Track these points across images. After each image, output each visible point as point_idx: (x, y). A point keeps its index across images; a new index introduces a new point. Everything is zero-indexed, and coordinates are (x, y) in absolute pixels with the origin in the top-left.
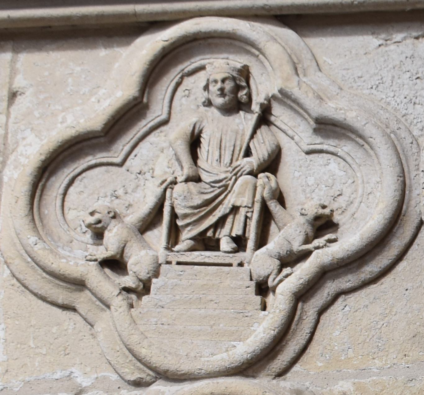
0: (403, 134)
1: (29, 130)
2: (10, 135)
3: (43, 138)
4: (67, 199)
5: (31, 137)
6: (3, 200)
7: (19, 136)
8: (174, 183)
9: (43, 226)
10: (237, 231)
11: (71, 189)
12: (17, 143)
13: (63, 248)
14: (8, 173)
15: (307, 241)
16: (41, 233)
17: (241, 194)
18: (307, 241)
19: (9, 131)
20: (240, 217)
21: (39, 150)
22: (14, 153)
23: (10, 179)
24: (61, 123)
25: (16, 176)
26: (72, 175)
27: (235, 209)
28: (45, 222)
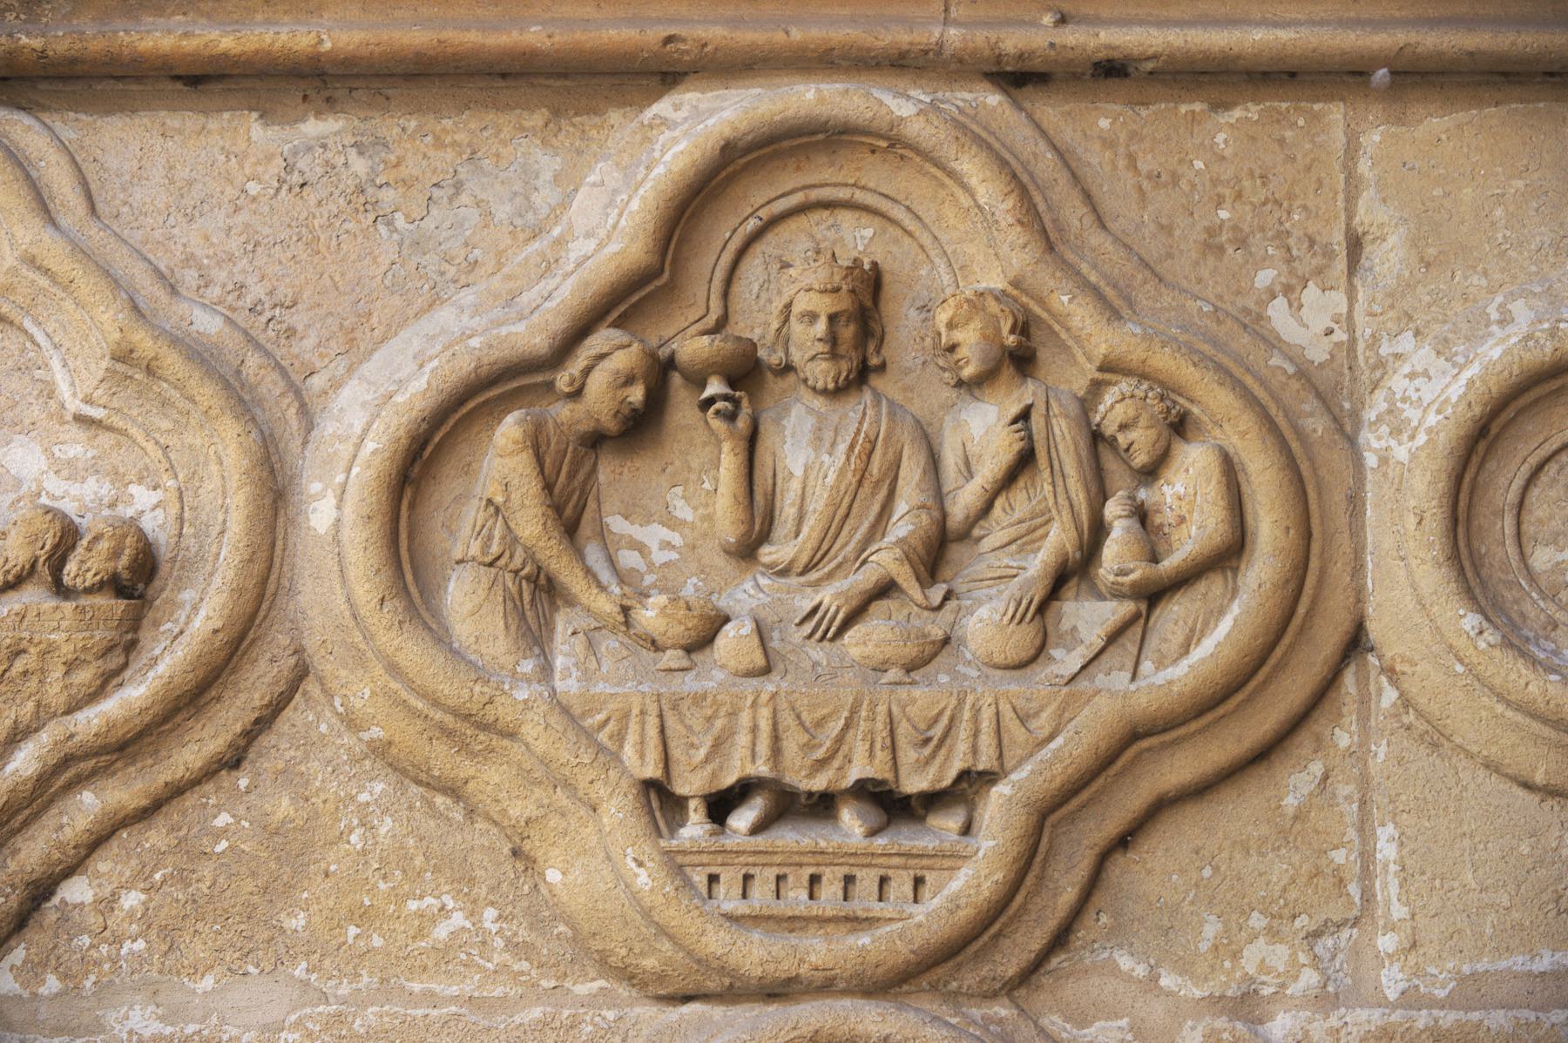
1: (1409, 334)
2: (1361, 346)
3: (1460, 359)
4: (1525, 517)
5: (1423, 356)
6: (1369, 513)
7: (1384, 350)
9: (1484, 585)
11: (1535, 492)
12: (1381, 364)
13: (1538, 645)
14: (1375, 444)
16: (1483, 603)
19: (1358, 333)
21: (1465, 394)
22: (1380, 395)
23: (1384, 460)
24: (1502, 322)
25: (1401, 453)
26: (1533, 460)
28: (1484, 572)
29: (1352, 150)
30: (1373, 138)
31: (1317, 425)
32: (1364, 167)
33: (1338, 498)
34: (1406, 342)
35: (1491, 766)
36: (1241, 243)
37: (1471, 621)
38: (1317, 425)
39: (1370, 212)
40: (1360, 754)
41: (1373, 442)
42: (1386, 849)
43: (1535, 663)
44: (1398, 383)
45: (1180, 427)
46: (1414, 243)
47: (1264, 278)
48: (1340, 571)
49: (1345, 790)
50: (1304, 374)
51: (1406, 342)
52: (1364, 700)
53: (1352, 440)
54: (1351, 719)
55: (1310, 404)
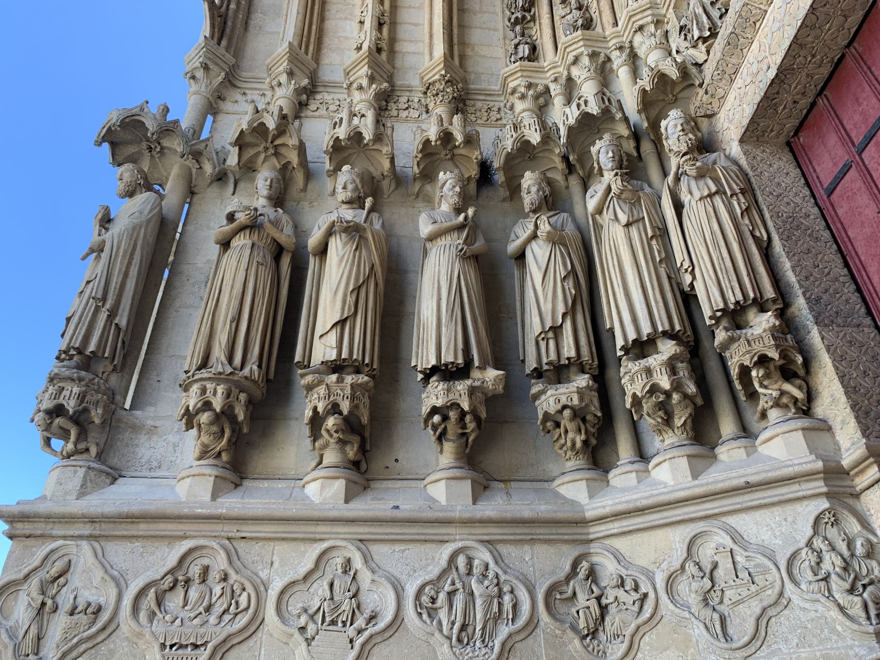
0: (399, 586)
5: (278, 579)
8: (325, 600)
10: (344, 619)
15: (367, 625)
17: (346, 606)
18: (367, 625)
20: (346, 612)
27: (344, 611)
29: (273, 550)
30: (276, 548)
31: (262, 589)
32: (275, 552)
33: (263, 600)
34: (276, 577)
35: (279, 640)
36: (257, 562)
37: (278, 618)
38: (262, 589)
39: (275, 558)
40: (261, 638)
41: (269, 591)
42: (263, 652)
43: (285, 624)
44: (274, 583)
45: (244, 589)
46: (280, 563)
47: (259, 567)
48: (262, 610)
49: (258, 643)
50: (262, 582)
51: (276, 577)
52: (263, 629)
53: (267, 591)
54: (261, 633)
55: (262, 586)
